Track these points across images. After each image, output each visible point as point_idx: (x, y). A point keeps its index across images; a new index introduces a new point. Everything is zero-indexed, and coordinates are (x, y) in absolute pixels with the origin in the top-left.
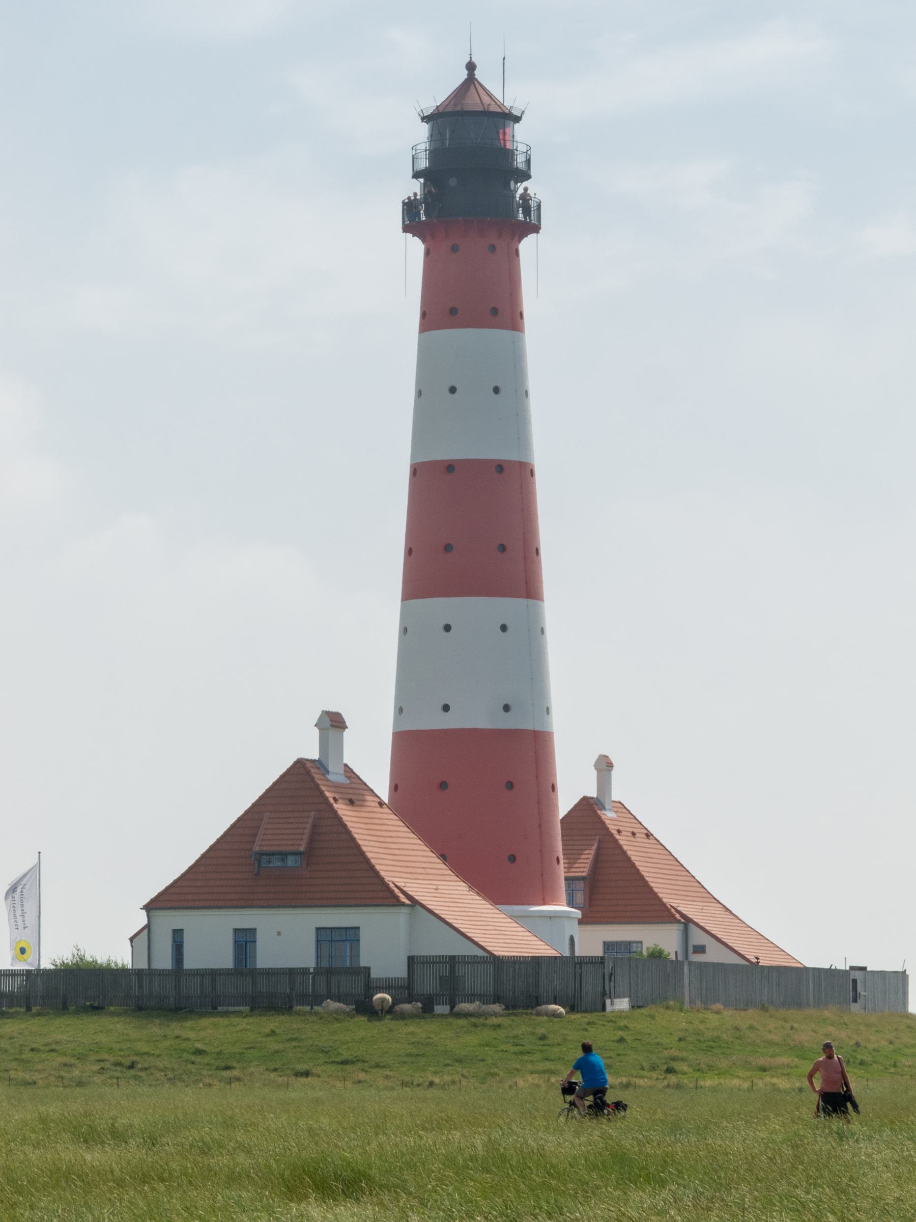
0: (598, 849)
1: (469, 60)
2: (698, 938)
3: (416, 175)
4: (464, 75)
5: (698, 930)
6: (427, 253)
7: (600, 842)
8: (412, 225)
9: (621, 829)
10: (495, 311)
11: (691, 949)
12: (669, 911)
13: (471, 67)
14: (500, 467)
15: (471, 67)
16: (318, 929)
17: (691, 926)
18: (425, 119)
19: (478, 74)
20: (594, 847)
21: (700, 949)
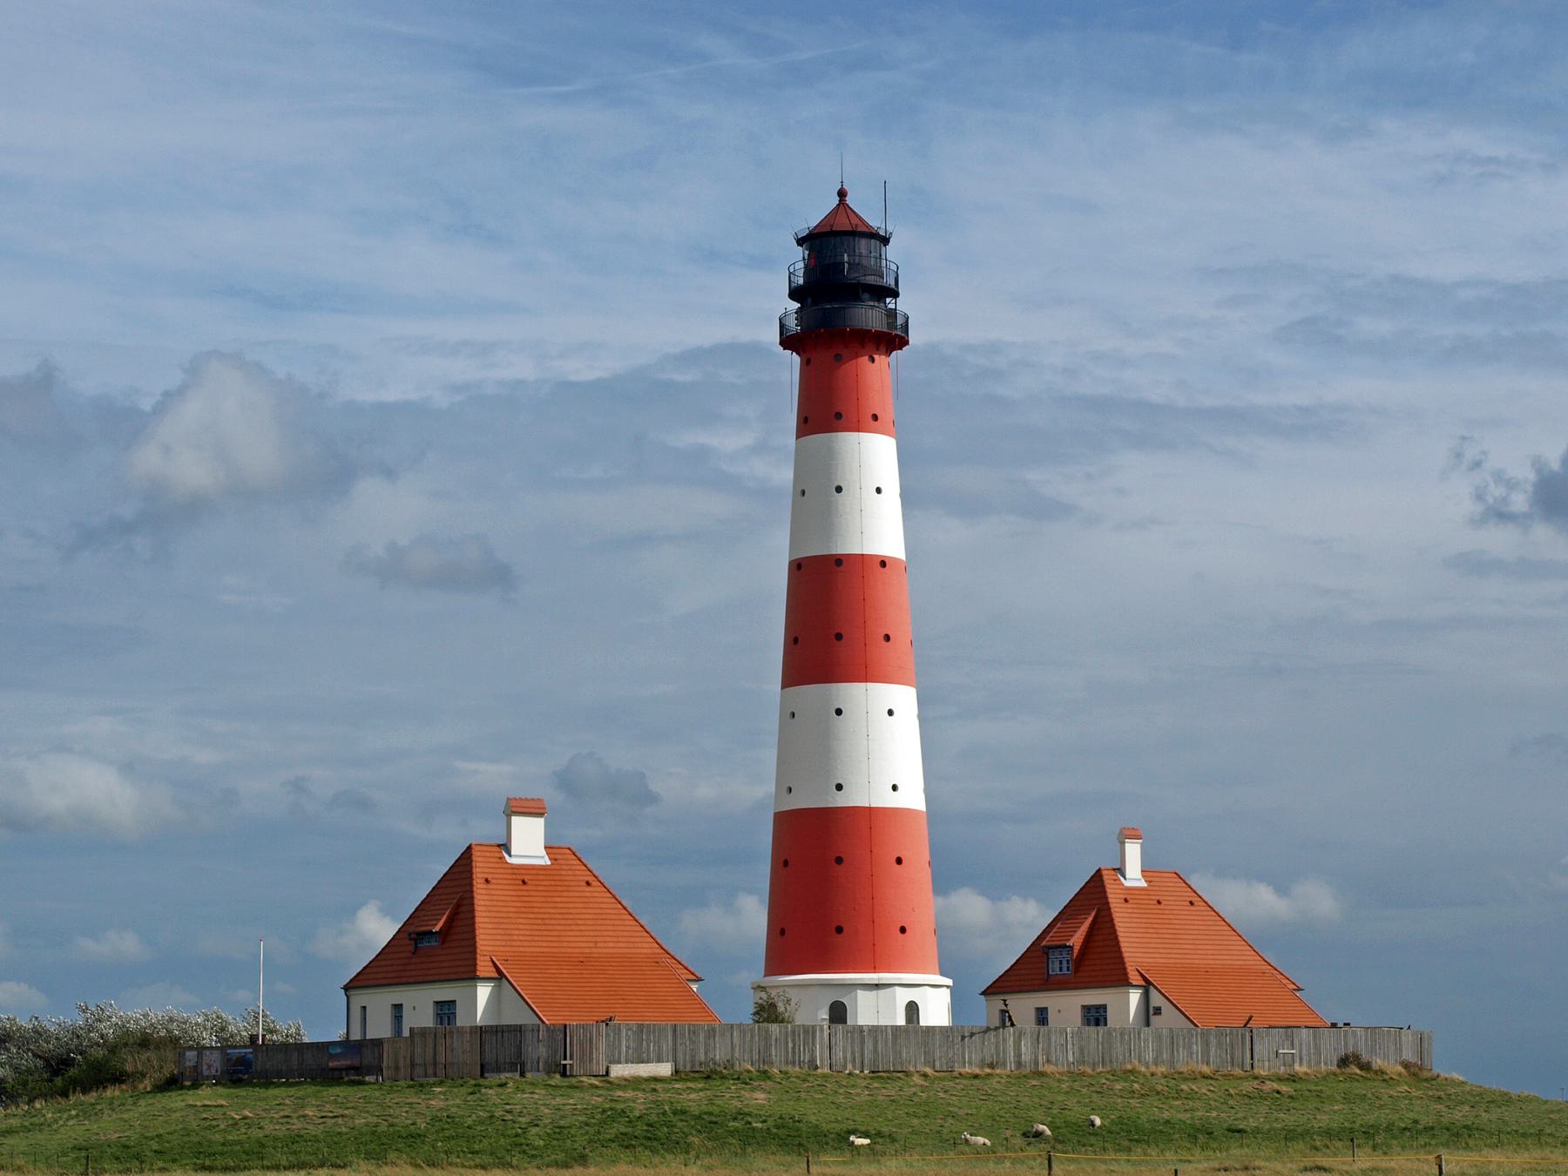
0: (1096, 917)
1: (840, 187)
2: (1156, 999)
3: (795, 294)
4: (836, 200)
5: (1157, 992)
6: (806, 363)
7: (1099, 910)
8: (788, 342)
9: (1160, 898)
10: (839, 416)
11: (1151, 1012)
12: (1126, 974)
13: (842, 194)
14: (839, 560)
15: (842, 194)
16: (437, 1003)
17: (1151, 988)
18: (800, 242)
19: (849, 200)
20: (1093, 914)
21: (1158, 1011)
